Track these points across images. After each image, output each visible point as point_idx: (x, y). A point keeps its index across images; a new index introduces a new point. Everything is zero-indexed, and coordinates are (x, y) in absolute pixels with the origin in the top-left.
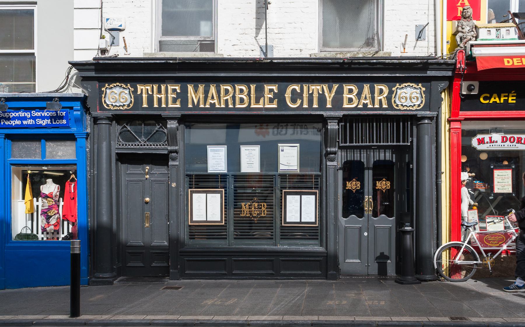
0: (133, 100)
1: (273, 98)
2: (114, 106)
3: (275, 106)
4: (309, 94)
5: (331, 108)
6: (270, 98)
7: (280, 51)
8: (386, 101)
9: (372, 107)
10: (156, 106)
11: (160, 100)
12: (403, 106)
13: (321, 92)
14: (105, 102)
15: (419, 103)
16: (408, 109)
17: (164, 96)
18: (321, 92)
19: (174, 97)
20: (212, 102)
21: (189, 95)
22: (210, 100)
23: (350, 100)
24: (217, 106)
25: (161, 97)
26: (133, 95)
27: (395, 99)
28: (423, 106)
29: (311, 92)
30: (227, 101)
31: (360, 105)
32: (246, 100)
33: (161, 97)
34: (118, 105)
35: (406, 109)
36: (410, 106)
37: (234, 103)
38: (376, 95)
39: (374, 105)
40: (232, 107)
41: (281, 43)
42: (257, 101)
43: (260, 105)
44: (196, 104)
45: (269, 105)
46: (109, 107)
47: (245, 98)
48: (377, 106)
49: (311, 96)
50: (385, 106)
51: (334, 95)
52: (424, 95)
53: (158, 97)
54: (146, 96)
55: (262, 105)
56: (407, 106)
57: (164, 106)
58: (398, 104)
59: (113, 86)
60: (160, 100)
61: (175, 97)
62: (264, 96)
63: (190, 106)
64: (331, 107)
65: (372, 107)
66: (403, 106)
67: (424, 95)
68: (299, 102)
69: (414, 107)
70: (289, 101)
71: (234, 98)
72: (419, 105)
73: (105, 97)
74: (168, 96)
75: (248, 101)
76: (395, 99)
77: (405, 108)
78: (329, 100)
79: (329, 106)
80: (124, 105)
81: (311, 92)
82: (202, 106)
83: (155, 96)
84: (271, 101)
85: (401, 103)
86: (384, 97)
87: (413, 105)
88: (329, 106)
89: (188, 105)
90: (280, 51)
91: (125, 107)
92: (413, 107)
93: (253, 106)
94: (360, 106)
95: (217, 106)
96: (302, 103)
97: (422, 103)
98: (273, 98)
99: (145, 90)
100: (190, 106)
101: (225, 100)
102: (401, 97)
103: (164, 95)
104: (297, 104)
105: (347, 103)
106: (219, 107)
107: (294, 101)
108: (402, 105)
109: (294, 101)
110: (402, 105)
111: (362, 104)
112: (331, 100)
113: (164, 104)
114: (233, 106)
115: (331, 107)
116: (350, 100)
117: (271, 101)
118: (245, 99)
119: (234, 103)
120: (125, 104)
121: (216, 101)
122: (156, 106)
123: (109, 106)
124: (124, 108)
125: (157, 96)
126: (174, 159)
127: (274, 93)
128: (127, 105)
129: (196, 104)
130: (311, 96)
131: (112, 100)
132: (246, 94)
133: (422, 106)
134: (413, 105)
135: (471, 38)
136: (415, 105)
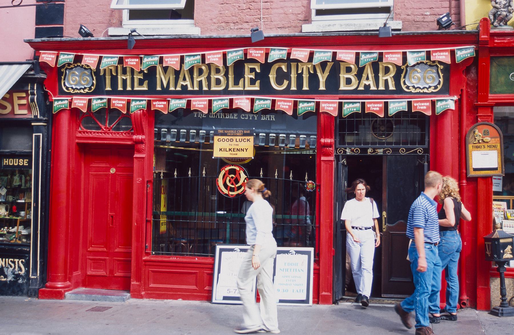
0: (95, 82)
1: (254, 78)
2: (74, 89)
3: (257, 88)
4: (297, 73)
5: (110, 90)
6: (251, 79)
7: (266, 23)
8: (393, 82)
9: (376, 89)
10: (120, 88)
11: (124, 82)
12: (416, 88)
13: (312, 72)
14: (65, 85)
15: (436, 84)
16: (421, 91)
17: (130, 77)
18: (312, 72)
19: (141, 78)
20: (184, 84)
21: (158, 76)
22: (182, 81)
23: (349, 81)
24: (190, 88)
25: (126, 79)
26: (95, 76)
27: (404, 79)
28: (440, 88)
29: (300, 72)
30: (200, 83)
31: (360, 87)
32: (223, 81)
33: (126, 79)
34: (79, 88)
35: (419, 92)
36: (424, 88)
37: (209, 86)
38: (380, 75)
39: (378, 86)
40: (207, 89)
41: (268, 14)
42: (236, 83)
43: (239, 87)
44: (165, 86)
45: (250, 87)
46: (69, 90)
47: (222, 79)
48: (382, 87)
49: (300, 77)
50: (392, 87)
51: (328, 75)
52: (443, 74)
53: (123, 79)
54: (109, 78)
55: (242, 88)
56: (420, 88)
57: (129, 88)
58: (409, 85)
59: (74, 66)
60: (124, 82)
61: (142, 78)
62: (244, 77)
63: (159, 88)
64: (308, 89)
65: (376, 89)
66: (416, 88)
67: (443, 74)
68: (286, 83)
69: (429, 89)
70: (274, 82)
71: (209, 79)
72: (436, 87)
73: (64, 79)
74: (134, 77)
75: (226, 82)
76: (404, 79)
77: (418, 90)
78: (322, 80)
79: (322, 87)
80: (85, 88)
81: (300, 72)
82: (172, 88)
83: (119, 77)
84: (252, 82)
85: (412, 85)
86: (390, 77)
87: (428, 87)
88: (322, 87)
89: (156, 87)
90: (266, 23)
91: (86, 90)
92: (428, 89)
93: (231, 88)
94: (361, 88)
95: (190, 88)
96: (289, 85)
97: (439, 83)
98: (254, 78)
99: (109, 70)
100: (159, 88)
101: (199, 81)
102: (412, 77)
103: (130, 76)
104: (283, 87)
105: (344, 84)
106: (192, 89)
107: (279, 82)
108: (414, 87)
109: (279, 82)
110: (414, 87)
111: (363, 85)
112: (324, 80)
113: (197, 87)
114: (123, 89)
115: (308, 89)
116: (349, 81)
117: (252, 82)
118: (221, 81)
119: (209, 86)
120: (86, 86)
121: (188, 83)
122: (120, 88)
123: (69, 89)
124: (85, 91)
125: (121, 78)
126: (139, 152)
127: (257, 74)
128: (89, 88)
129: (165, 86)
130: (300, 77)
131: (72, 82)
132: (222, 74)
133: (439, 87)
134: (428, 87)
135: (508, 15)
136: (430, 87)
